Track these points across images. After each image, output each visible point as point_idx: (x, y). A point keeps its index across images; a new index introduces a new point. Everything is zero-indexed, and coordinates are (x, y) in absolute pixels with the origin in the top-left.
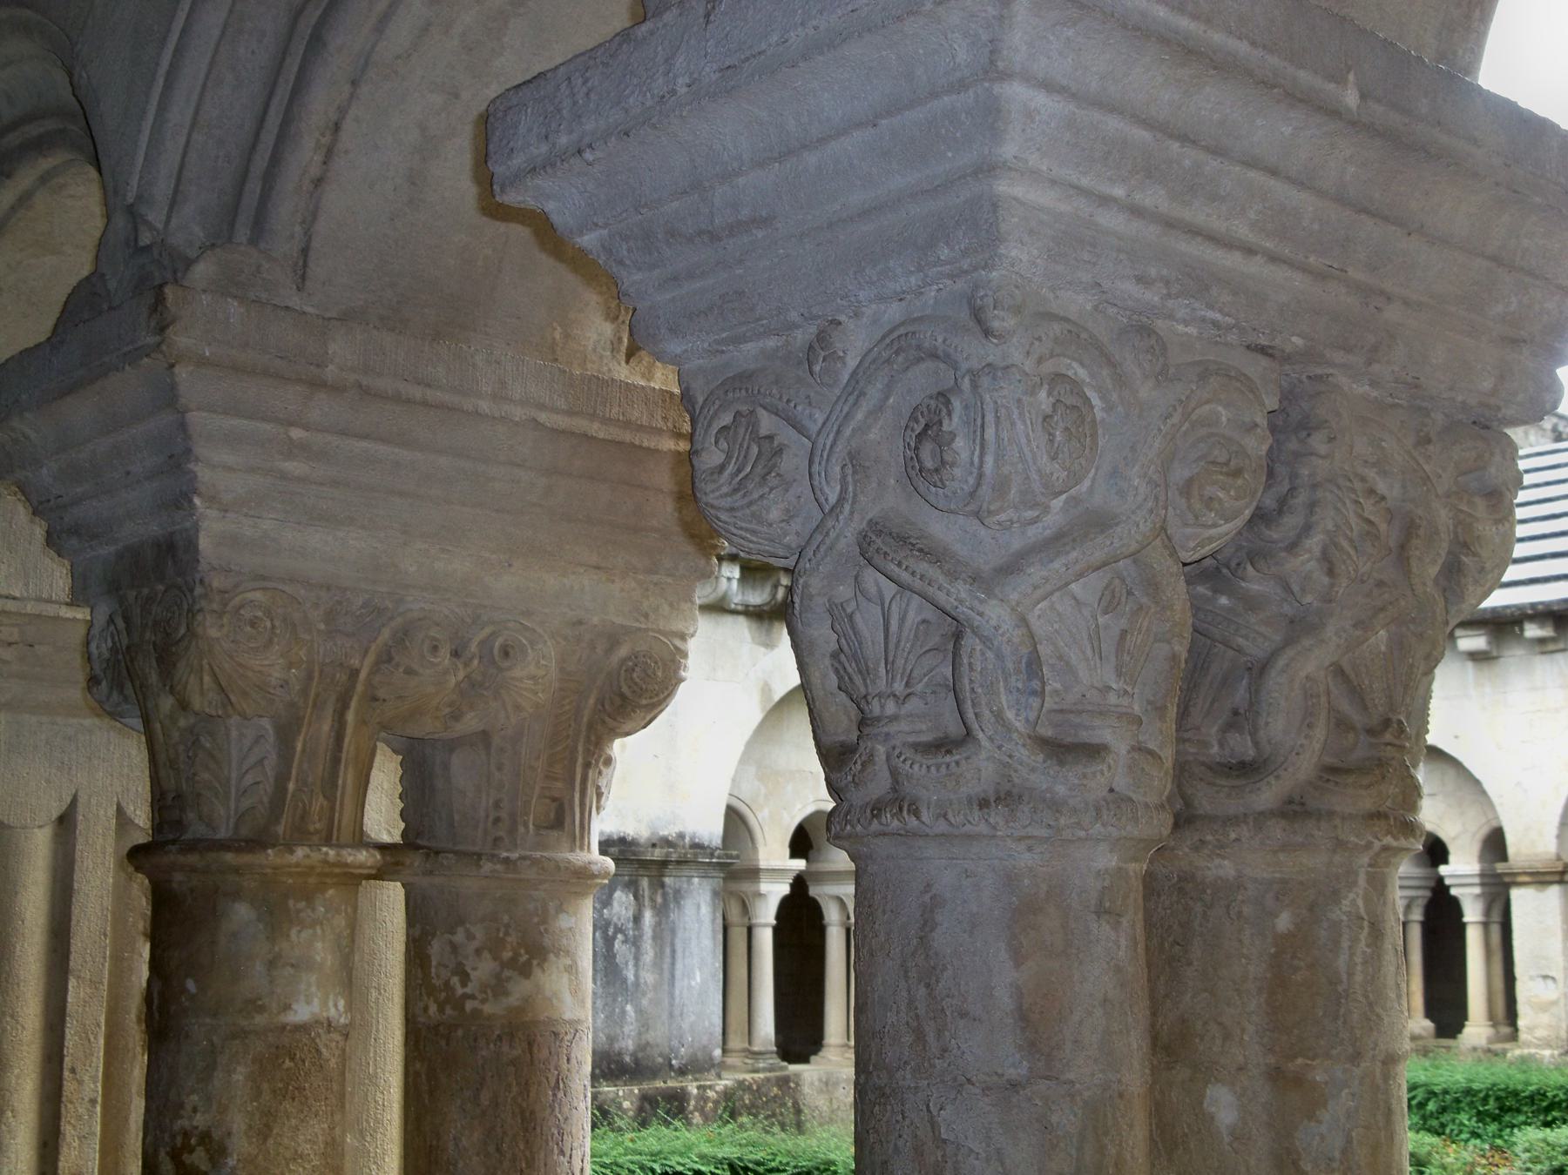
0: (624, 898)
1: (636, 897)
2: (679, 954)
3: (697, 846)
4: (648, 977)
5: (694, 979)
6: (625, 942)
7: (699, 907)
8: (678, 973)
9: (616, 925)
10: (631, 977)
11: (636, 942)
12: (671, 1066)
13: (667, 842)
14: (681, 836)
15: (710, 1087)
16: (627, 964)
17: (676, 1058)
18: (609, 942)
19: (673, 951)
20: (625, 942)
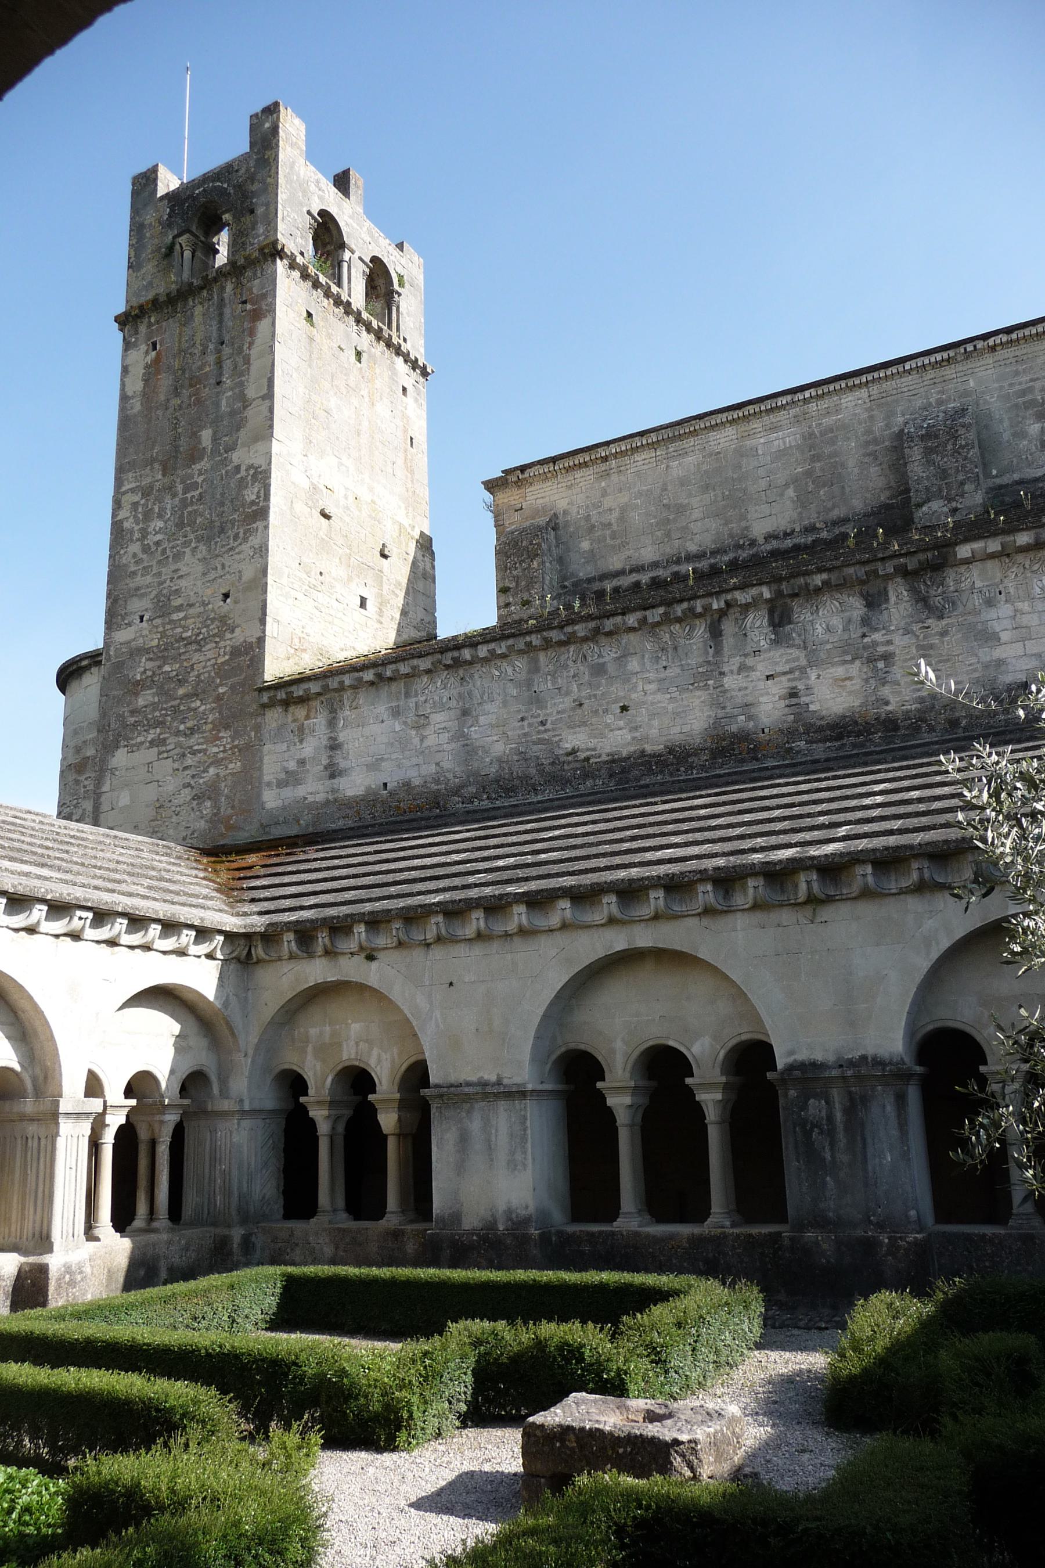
0: (817, 1104)
1: (827, 1103)
2: (869, 1141)
3: (878, 1062)
4: (844, 1158)
5: (885, 1158)
6: (821, 1133)
7: (884, 1107)
8: (869, 1155)
9: (812, 1123)
10: (828, 1156)
11: (831, 1133)
12: (870, 1222)
13: (851, 1063)
14: (864, 1058)
15: (901, 1238)
16: (824, 1148)
17: (874, 1215)
18: (808, 1134)
19: (864, 1140)
20: (821, 1133)
